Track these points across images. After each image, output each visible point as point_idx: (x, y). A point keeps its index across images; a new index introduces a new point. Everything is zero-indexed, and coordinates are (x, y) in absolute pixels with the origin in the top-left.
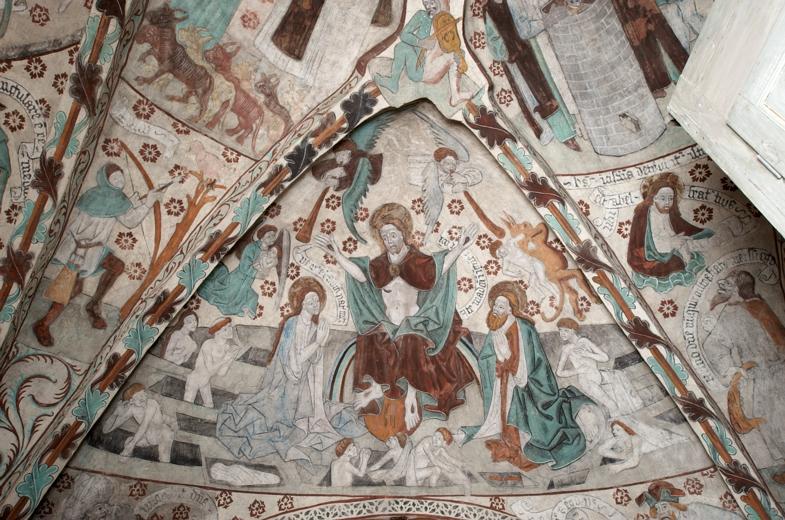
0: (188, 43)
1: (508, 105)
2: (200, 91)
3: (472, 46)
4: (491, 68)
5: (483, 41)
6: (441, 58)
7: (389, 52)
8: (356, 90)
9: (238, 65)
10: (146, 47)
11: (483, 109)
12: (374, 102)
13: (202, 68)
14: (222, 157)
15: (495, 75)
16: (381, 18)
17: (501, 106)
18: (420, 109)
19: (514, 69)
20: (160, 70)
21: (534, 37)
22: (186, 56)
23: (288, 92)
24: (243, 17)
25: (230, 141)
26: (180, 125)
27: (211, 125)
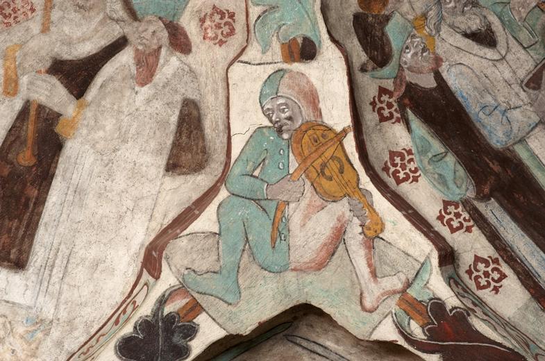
1: (496, 290)
3: (391, 181)
4: (440, 218)
5: (412, 166)
6: (322, 213)
7: (206, 221)
8: (146, 310)
11: (438, 306)
12: (191, 331)
15: (453, 230)
16: (186, 158)
17: (480, 293)
18: (304, 330)
19: (493, 211)
21: (522, 141)
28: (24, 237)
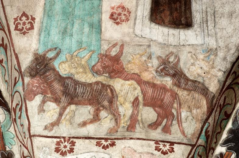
0: (73, 71)
2: (106, 103)
9: (129, 62)
10: (38, 99)
13: (97, 83)
14: (156, 152)
20: (61, 109)
22: (77, 83)
23: (193, 64)
24: (112, 15)
25: (157, 134)
26: (103, 142)
27: (131, 127)
28: (185, 10)
